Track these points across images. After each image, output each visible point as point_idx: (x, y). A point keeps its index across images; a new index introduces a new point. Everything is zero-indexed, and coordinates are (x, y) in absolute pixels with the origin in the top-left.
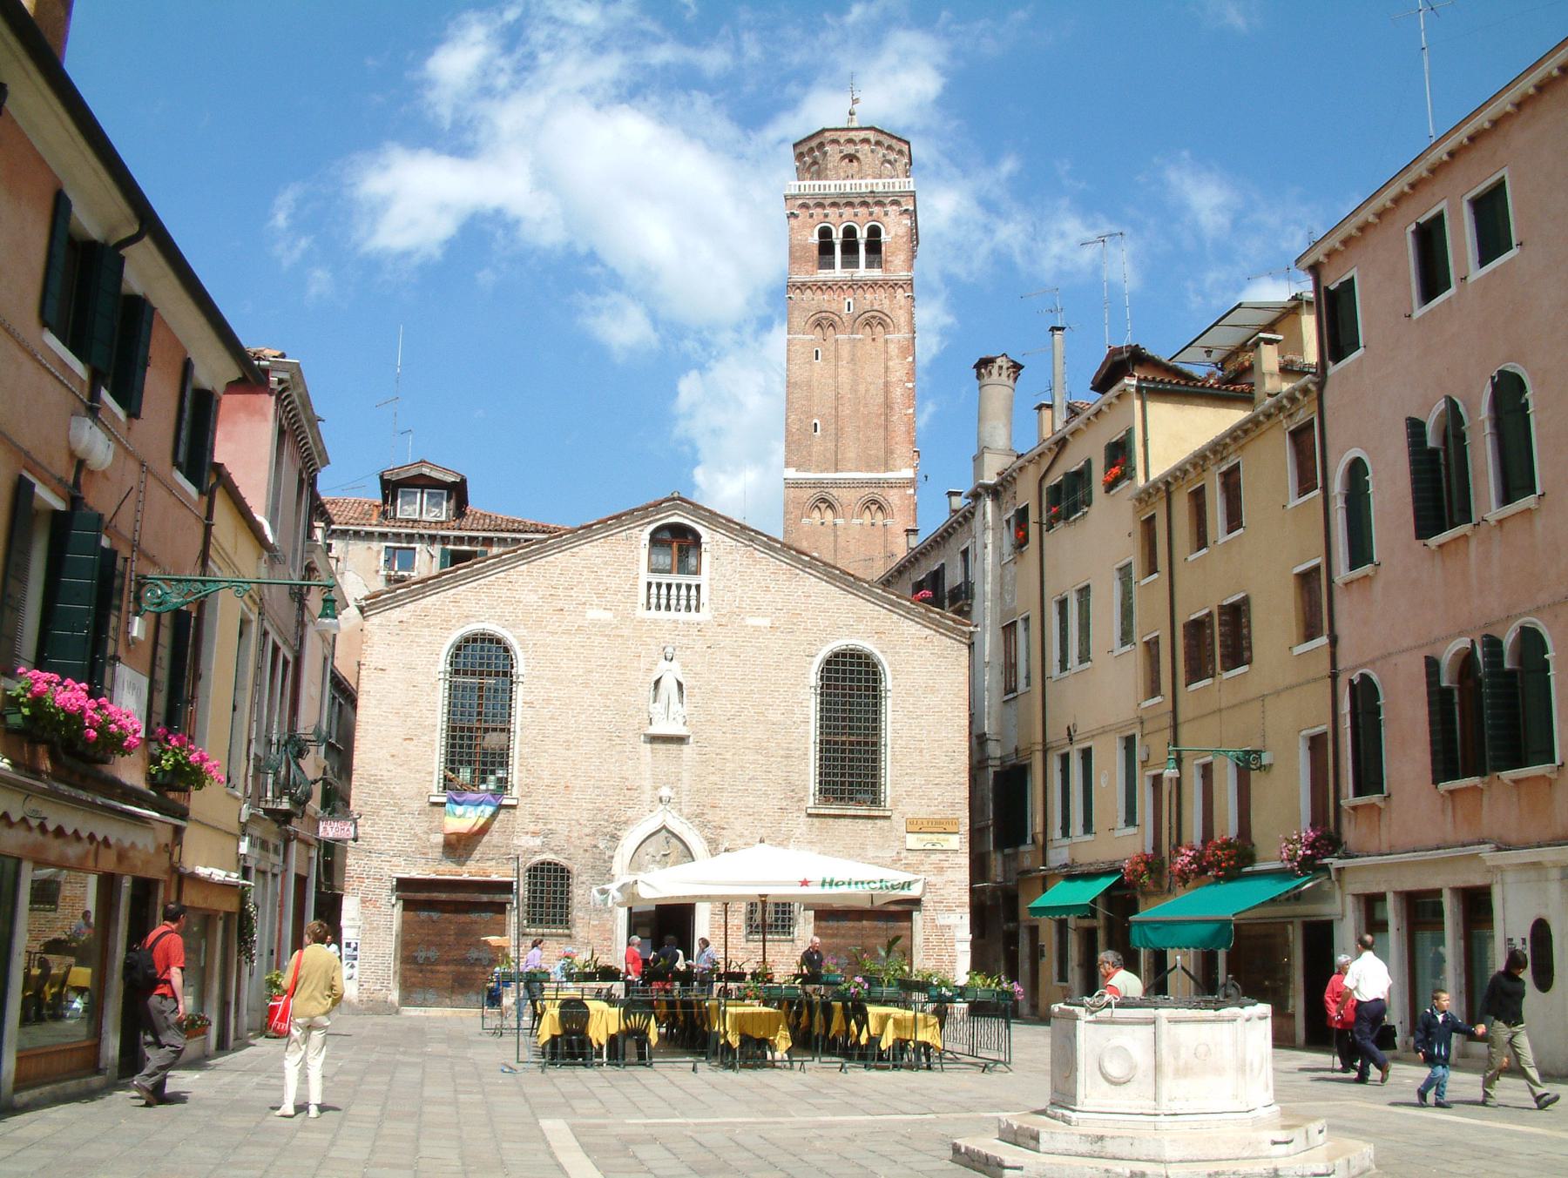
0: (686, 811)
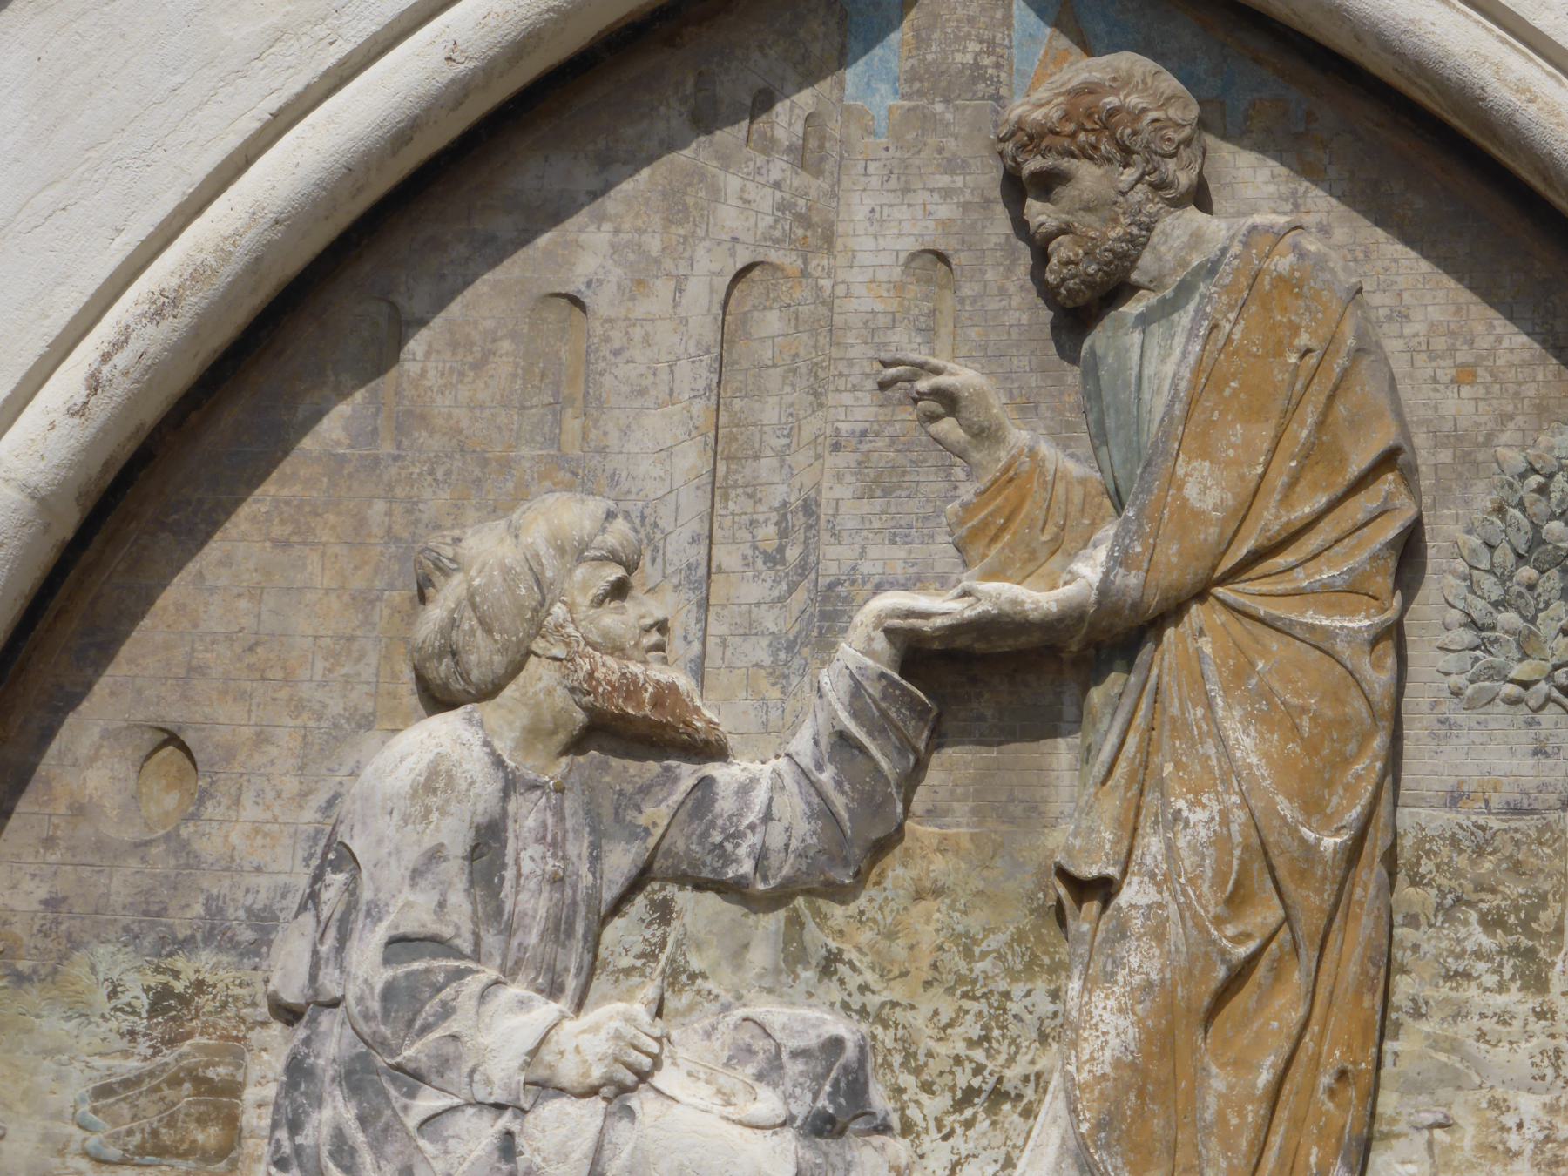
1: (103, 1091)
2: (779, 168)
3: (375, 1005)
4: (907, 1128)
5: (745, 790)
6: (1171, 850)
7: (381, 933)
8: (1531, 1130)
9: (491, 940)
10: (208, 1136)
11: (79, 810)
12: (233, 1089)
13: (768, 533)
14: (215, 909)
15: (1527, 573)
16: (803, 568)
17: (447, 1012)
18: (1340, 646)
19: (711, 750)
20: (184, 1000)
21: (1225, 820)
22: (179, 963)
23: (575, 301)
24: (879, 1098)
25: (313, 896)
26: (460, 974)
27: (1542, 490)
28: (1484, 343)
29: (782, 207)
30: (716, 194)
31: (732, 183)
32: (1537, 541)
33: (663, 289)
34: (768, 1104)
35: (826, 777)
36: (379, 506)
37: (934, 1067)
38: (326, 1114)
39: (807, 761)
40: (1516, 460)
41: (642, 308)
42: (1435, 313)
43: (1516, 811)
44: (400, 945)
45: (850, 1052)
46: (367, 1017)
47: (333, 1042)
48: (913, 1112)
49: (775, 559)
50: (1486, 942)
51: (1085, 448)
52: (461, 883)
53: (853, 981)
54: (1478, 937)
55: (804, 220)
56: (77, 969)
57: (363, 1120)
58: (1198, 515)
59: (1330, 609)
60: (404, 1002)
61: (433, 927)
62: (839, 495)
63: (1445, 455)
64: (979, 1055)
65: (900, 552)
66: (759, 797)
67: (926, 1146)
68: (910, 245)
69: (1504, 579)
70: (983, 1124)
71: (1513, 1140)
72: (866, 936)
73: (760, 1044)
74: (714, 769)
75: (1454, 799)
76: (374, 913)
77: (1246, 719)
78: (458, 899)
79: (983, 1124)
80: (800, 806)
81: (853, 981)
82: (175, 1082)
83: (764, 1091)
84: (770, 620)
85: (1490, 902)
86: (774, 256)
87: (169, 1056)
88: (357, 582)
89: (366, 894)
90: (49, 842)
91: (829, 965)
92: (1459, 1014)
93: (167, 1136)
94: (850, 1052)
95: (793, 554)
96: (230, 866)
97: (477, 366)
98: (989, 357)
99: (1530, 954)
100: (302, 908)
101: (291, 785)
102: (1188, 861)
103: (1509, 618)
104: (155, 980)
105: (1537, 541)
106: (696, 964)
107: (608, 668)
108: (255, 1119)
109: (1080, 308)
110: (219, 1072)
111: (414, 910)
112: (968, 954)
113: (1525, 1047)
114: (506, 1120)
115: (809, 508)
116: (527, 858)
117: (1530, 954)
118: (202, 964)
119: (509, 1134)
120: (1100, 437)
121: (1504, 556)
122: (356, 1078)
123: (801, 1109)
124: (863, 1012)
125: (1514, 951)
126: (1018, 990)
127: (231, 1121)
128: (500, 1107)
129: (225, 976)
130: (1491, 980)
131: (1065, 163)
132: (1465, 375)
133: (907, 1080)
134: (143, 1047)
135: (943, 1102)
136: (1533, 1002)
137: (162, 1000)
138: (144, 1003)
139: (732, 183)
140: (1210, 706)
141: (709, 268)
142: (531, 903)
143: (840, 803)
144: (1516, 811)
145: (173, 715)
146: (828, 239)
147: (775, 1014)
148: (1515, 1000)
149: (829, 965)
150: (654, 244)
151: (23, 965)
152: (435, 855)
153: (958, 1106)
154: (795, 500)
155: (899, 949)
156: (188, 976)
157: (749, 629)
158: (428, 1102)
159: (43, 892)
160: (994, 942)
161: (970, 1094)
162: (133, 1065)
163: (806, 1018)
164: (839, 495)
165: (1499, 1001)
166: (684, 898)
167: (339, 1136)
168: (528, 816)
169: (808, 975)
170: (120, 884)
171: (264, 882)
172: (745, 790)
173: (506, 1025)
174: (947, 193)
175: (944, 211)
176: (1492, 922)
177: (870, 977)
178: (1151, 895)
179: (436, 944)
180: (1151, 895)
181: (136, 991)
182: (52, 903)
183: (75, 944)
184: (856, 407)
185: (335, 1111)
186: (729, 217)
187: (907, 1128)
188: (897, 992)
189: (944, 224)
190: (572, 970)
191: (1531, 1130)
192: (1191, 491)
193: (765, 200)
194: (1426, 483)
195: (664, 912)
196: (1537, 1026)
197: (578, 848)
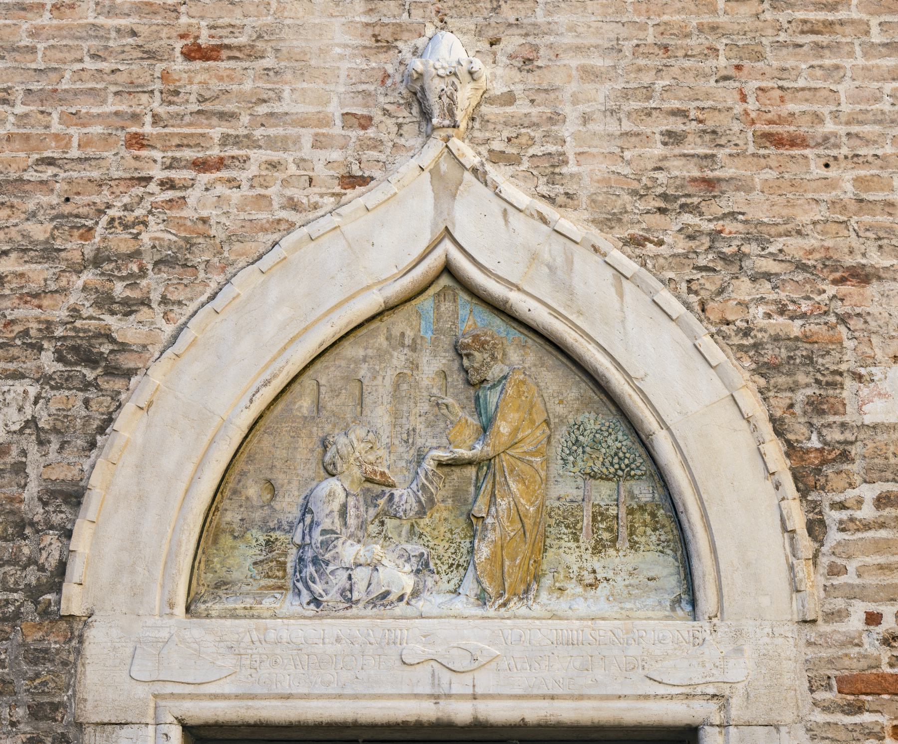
0: (587, 172)
1: (255, 563)
2: (406, 351)
3: (319, 545)
4: (438, 573)
5: (401, 496)
6: (497, 511)
7: (320, 529)
8: (575, 573)
9: (344, 530)
10: (280, 574)
11: (247, 498)
12: (285, 563)
13: (405, 436)
14: (279, 522)
15: (575, 448)
16: (413, 444)
17: (335, 547)
18: (534, 464)
19: (393, 486)
20: (273, 542)
21: (509, 502)
22: (272, 534)
23: (359, 380)
24: (432, 566)
25: (303, 519)
26: (337, 538)
27: (578, 429)
28: (565, 395)
29: (407, 360)
30: (392, 356)
31: (395, 354)
32: (577, 441)
33: (380, 378)
34: (408, 568)
35: (420, 494)
36: (315, 429)
37: (444, 559)
38: (308, 569)
39: (415, 490)
40: (572, 422)
41: (375, 383)
42: (554, 388)
43: (572, 501)
44: (324, 532)
45: (426, 556)
46: (317, 548)
47: (309, 554)
48: (439, 569)
49: (407, 442)
50: (566, 531)
51: (476, 417)
52: (337, 517)
53: (426, 539)
54: (564, 530)
55: (412, 363)
56: (248, 535)
57: (316, 571)
58: (503, 434)
59: (532, 456)
60: (325, 545)
61: (331, 527)
62: (421, 427)
63: (557, 420)
64: (454, 556)
65: (435, 440)
66: (404, 498)
68: (436, 369)
69: (570, 449)
70: (455, 572)
71: (572, 575)
72: (428, 529)
73: (405, 554)
74: (394, 491)
75: (559, 499)
76: (318, 524)
77: (513, 482)
78: (336, 520)
79: (455, 572)
80: (414, 500)
81: (426, 539)
82: (272, 561)
83: (406, 564)
84: (405, 456)
85: (567, 522)
86: (405, 371)
87: (270, 555)
88: (310, 446)
89: (315, 519)
90: (241, 506)
91: (421, 536)
92: (560, 548)
93: (270, 574)
94: (426, 556)
95: (411, 441)
96: (283, 511)
97: (337, 396)
98: (455, 396)
99: (575, 534)
100: (300, 522)
101: (296, 493)
102: (501, 514)
103: (571, 458)
104: (266, 538)
105: (577, 441)
106: (390, 536)
107: (369, 468)
108: (290, 570)
109: (475, 384)
110: (282, 559)
111: (326, 524)
112: (451, 533)
113: (574, 555)
114: (349, 572)
115: (414, 430)
116: (352, 512)
117: (575, 534)
118: (278, 534)
119: (350, 575)
120: (480, 415)
121: (570, 444)
122: (315, 561)
123: (415, 569)
124: (428, 546)
125: (572, 533)
126: (462, 541)
127: (285, 570)
128: (347, 569)
129: (283, 537)
130: (567, 539)
131: (472, 352)
132: (561, 402)
133: (438, 561)
134: (264, 553)
135: (447, 567)
136: (576, 544)
137: (268, 542)
138: (264, 543)
139: (395, 354)
140: (506, 478)
141: (390, 375)
142: (352, 521)
143: (423, 499)
144: (572, 501)
145: (269, 477)
146: (417, 367)
147: (409, 547)
148: (573, 545)
149: (421, 536)
150: (377, 368)
151: (236, 534)
152: (332, 512)
153: (449, 568)
154: (411, 428)
155: (436, 533)
156: (274, 537)
157: (401, 459)
158: (331, 568)
159: (240, 517)
160: (458, 531)
161: (452, 565)
162: (262, 558)
163: (415, 548)
164: (421, 427)
165: (569, 544)
166: (387, 521)
167: (311, 574)
168: (351, 502)
169: (416, 538)
170: (258, 515)
171: (290, 515)
172: (401, 496)
173: (349, 551)
174: (445, 357)
175: (444, 361)
176: (567, 527)
177: (430, 538)
178: (493, 521)
179: (333, 532)
180: (493, 521)
181: (262, 539)
182: (242, 520)
183: (248, 530)
184: (425, 407)
185: (311, 569)
186: (395, 362)
187: (438, 573)
188: (436, 542)
189: (444, 364)
190: (361, 535)
191: (575, 573)
192: (501, 429)
193: (403, 358)
194: (552, 426)
195: (382, 523)
196: (577, 550)
197: (362, 509)
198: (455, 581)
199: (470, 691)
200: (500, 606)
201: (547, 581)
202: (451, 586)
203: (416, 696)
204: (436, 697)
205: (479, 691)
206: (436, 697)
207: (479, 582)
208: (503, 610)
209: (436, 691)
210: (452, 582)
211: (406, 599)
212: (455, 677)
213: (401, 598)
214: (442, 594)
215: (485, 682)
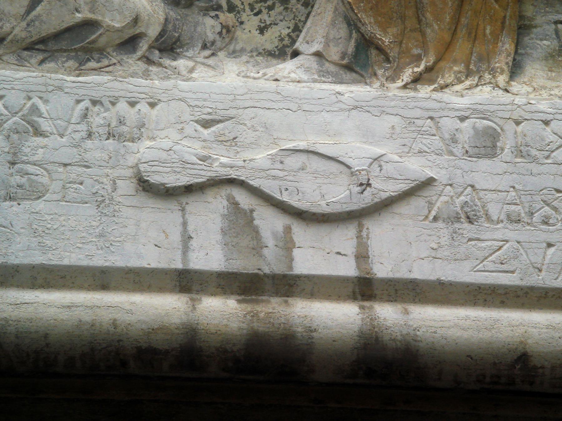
67: (244, 17)
198: (284, 29)
199: (347, 268)
200: (417, 80)
201: (542, 42)
202: (270, 40)
203: (186, 281)
204: (246, 285)
205: (382, 270)
206: (246, 285)
207: (352, 24)
208: (425, 91)
209: (243, 264)
210: (272, 34)
211: (143, 46)
212: (301, 233)
213: (129, 43)
214: (244, 58)
215: (400, 248)
